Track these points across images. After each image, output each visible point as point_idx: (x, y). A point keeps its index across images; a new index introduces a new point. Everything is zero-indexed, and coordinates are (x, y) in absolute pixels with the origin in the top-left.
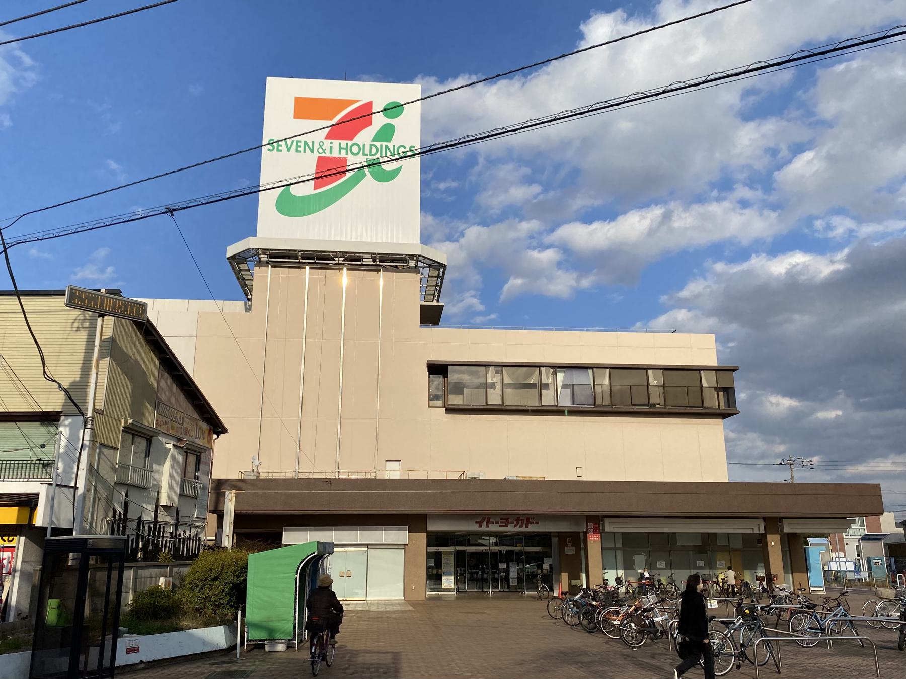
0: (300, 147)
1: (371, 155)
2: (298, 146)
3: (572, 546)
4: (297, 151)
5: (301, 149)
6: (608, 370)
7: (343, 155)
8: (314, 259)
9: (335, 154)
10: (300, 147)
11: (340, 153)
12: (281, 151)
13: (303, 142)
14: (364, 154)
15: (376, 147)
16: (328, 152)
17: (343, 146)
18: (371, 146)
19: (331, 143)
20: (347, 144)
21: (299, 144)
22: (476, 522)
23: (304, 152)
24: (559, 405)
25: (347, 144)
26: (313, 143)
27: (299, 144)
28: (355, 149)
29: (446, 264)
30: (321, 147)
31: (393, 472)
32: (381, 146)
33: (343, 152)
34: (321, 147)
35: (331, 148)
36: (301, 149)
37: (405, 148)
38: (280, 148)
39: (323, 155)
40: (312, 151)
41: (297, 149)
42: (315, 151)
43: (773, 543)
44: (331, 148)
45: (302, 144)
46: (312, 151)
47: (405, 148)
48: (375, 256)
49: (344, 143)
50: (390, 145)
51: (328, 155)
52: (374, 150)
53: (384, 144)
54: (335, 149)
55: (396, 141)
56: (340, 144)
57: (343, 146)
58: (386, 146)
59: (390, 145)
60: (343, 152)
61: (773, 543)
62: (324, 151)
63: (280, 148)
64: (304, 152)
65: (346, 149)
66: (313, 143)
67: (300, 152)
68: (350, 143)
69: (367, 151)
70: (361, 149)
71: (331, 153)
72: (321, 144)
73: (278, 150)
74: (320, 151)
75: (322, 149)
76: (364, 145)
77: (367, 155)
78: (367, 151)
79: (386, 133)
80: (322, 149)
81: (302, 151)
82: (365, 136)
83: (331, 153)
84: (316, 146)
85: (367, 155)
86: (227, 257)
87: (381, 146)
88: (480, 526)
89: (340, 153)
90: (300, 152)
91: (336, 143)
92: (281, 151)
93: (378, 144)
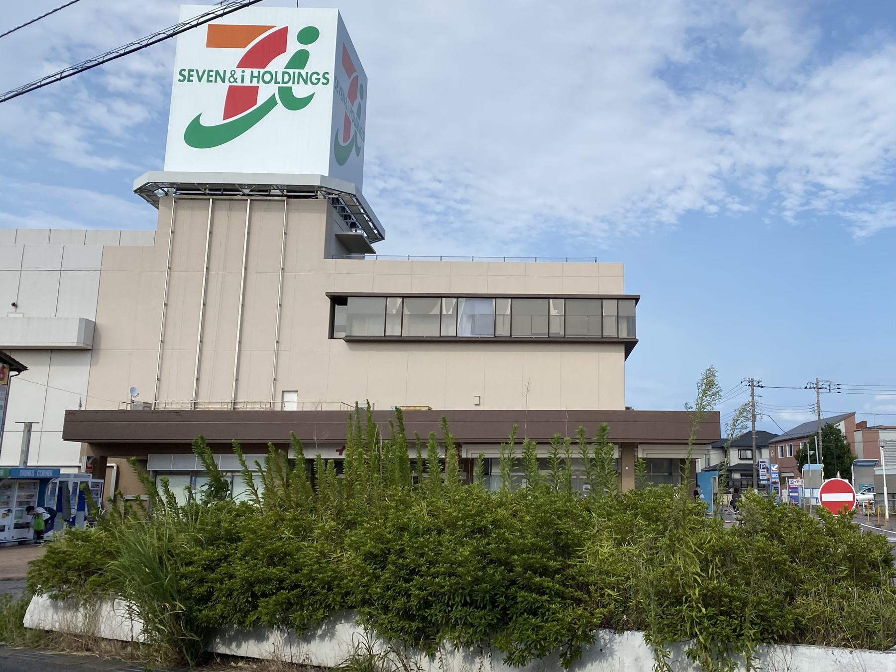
0: (212, 76)
1: (283, 82)
2: (209, 76)
3: (464, 472)
4: (208, 81)
5: (213, 79)
6: (510, 300)
7: (255, 83)
8: (220, 190)
9: (247, 83)
10: (212, 76)
11: (251, 82)
12: (192, 81)
13: (214, 71)
14: (276, 82)
15: (288, 73)
16: (239, 81)
17: (255, 74)
18: (284, 73)
19: (243, 72)
20: (259, 72)
21: (211, 73)
22: (337, 451)
23: (216, 81)
24: (458, 335)
25: (259, 72)
26: (225, 71)
27: (211, 73)
28: (267, 77)
29: (354, 194)
30: (232, 76)
31: (292, 404)
32: (294, 73)
33: (255, 80)
34: (232, 76)
35: (243, 76)
36: (213, 79)
37: (318, 74)
38: (191, 78)
39: (235, 84)
40: (223, 80)
41: (208, 78)
42: (227, 80)
43: (627, 468)
44: (243, 76)
45: (213, 74)
46: (223, 80)
47: (318, 74)
48: (281, 187)
49: (256, 71)
50: (303, 72)
51: (239, 84)
52: (286, 77)
53: (297, 71)
54: (246, 77)
55: (309, 68)
56: (252, 72)
57: (255, 74)
58: (300, 74)
59: (303, 72)
60: (255, 80)
61: (627, 468)
62: (235, 80)
63: (191, 78)
64: (216, 81)
65: (258, 77)
66: (225, 71)
67: (211, 81)
68: (262, 71)
69: (279, 79)
70: (274, 77)
71: (242, 82)
72: (233, 73)
73: (189, 81)
74: (232, 80)
75: (234, 78)
76: (276, 72)
77: (279, 83)
78: (279, 79)
79: (300, 59)
80: (234, 78)
81: (213, 81)
82: (278, 64)
83: (242, 82)
84: (228, 75)
85: (279, 83)
86: (134, 189)
87: (294, 73)
88: (341, 454)
89: (251, 82)
90: (211, 81)
91: (248, 71)
92: (192, 81)
93: (291, 71)
